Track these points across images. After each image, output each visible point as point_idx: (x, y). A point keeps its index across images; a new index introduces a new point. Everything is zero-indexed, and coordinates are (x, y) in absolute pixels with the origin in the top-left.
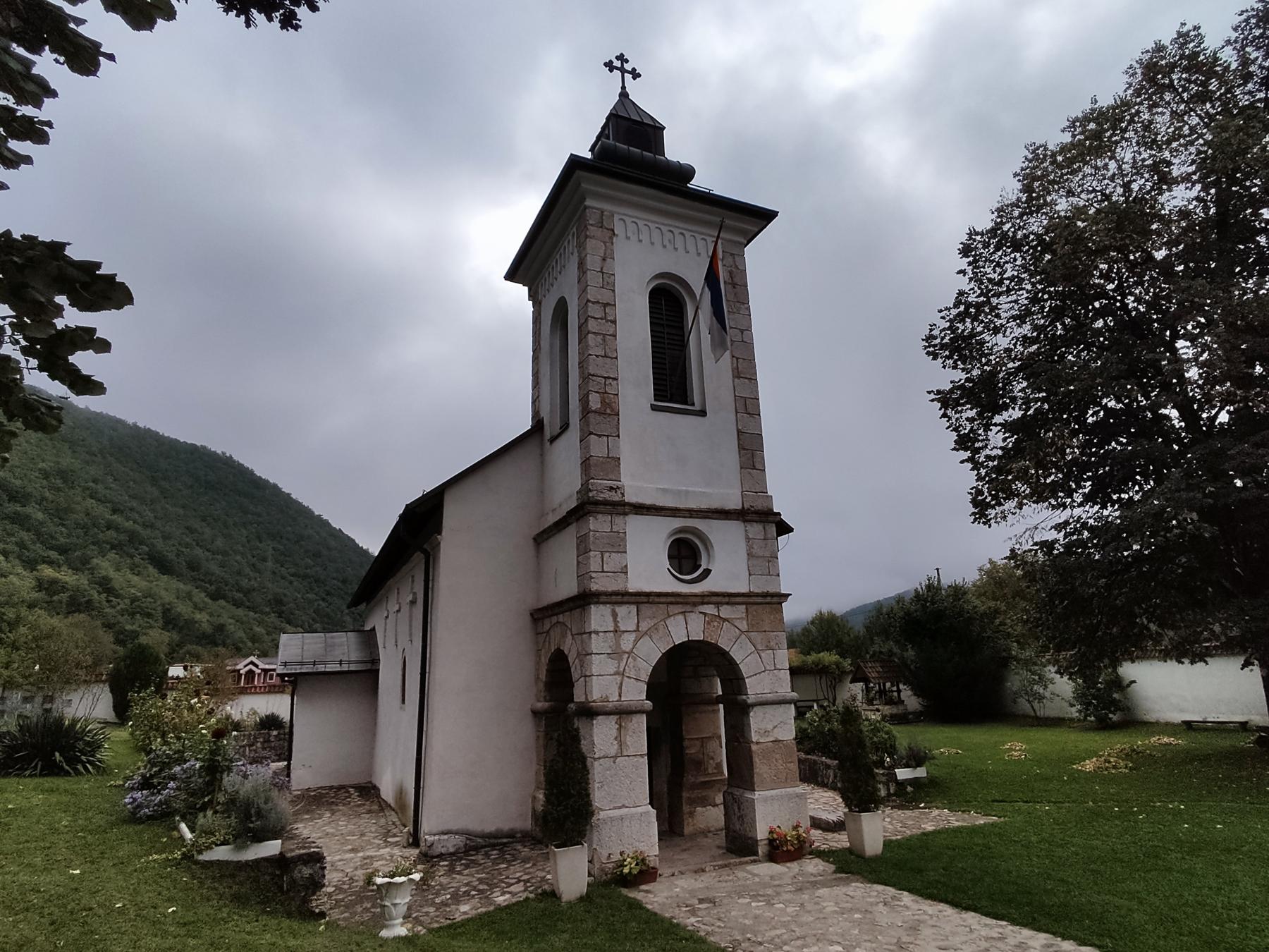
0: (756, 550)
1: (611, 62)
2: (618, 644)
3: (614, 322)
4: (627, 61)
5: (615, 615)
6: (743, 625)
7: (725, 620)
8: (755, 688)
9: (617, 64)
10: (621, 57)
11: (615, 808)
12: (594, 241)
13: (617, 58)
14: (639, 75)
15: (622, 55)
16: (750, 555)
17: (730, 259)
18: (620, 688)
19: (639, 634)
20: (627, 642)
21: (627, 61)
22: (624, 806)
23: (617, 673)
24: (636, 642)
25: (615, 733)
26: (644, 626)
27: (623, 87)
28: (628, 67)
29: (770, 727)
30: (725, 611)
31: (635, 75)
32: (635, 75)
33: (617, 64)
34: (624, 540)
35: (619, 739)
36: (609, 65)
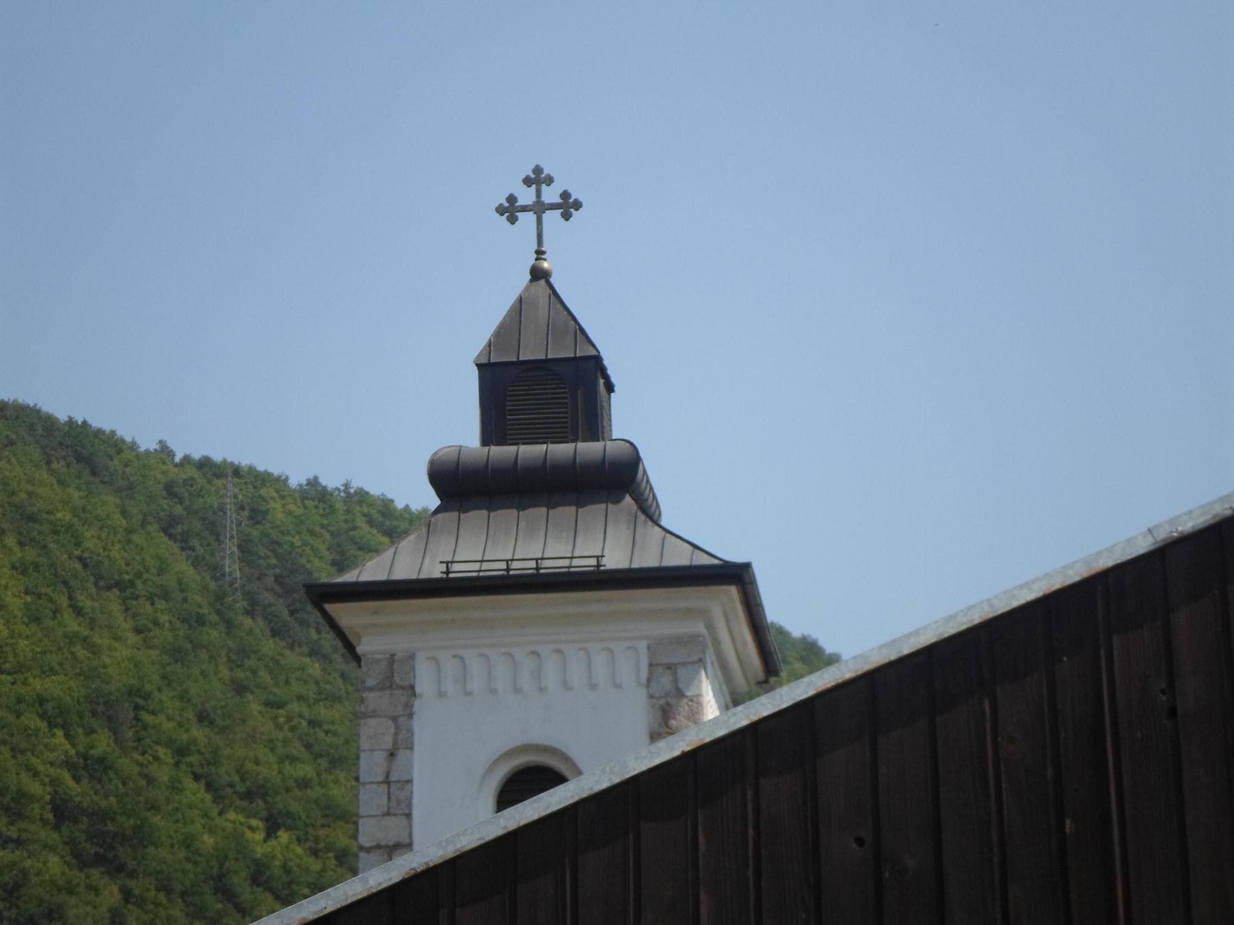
1: (512, 199)
4: (550, 180)
9: (526, 196)
10: (537, 179)
12: (372, 722)
13: (528, 181)
14: (577, 205)
15: (538, 170)
17: (665, 681)
21: (550, 180)
27: (540, 253)
28: (551, 195)
31: (568, 206)
32: (568, 206)
33: (526, 196)
36: (510, 210)
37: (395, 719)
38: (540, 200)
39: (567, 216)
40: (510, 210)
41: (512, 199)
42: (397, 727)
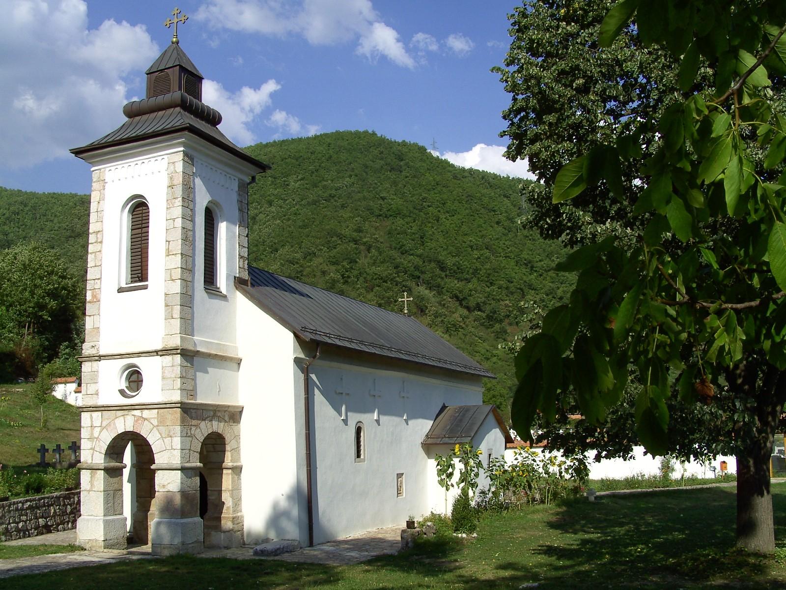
0: (167, 375)
2: (92, 434)
3: (101, 242)
5: (91, 417)
6: (155, 422)
7: (145, 419)
8: (160, 459)
11: (89, 515)
16: (163, 378)
17: (172, 167)
18: (92, 456)
19: (102, 428)
20: (96, 432)
22: (91, 516)
23: (91, 449)
24: (100, 432)
25: (89, 479)
26: (104, 424)
29: (166, 483)
30: (146, 414)
34: (97, 376)
35: (91, 482)
37: (100, 191)
42: (101, 194)
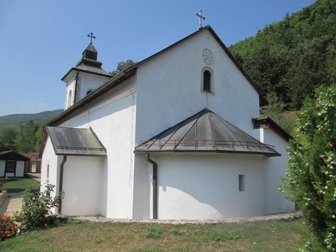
1: (89, 35)
4: (93, 34)
9: (90, 35)
10: (92, 34)
13: (91, 34)
14: (95, 38)
15: (92, 33)
21: (93, 34)
27: (91, 41)
31: (94, 37)
32: (94, 37)
36: (89, 36)
38: (91, 36)
39: (94, 38)
40: (89, 36)
41: (89, 35)
